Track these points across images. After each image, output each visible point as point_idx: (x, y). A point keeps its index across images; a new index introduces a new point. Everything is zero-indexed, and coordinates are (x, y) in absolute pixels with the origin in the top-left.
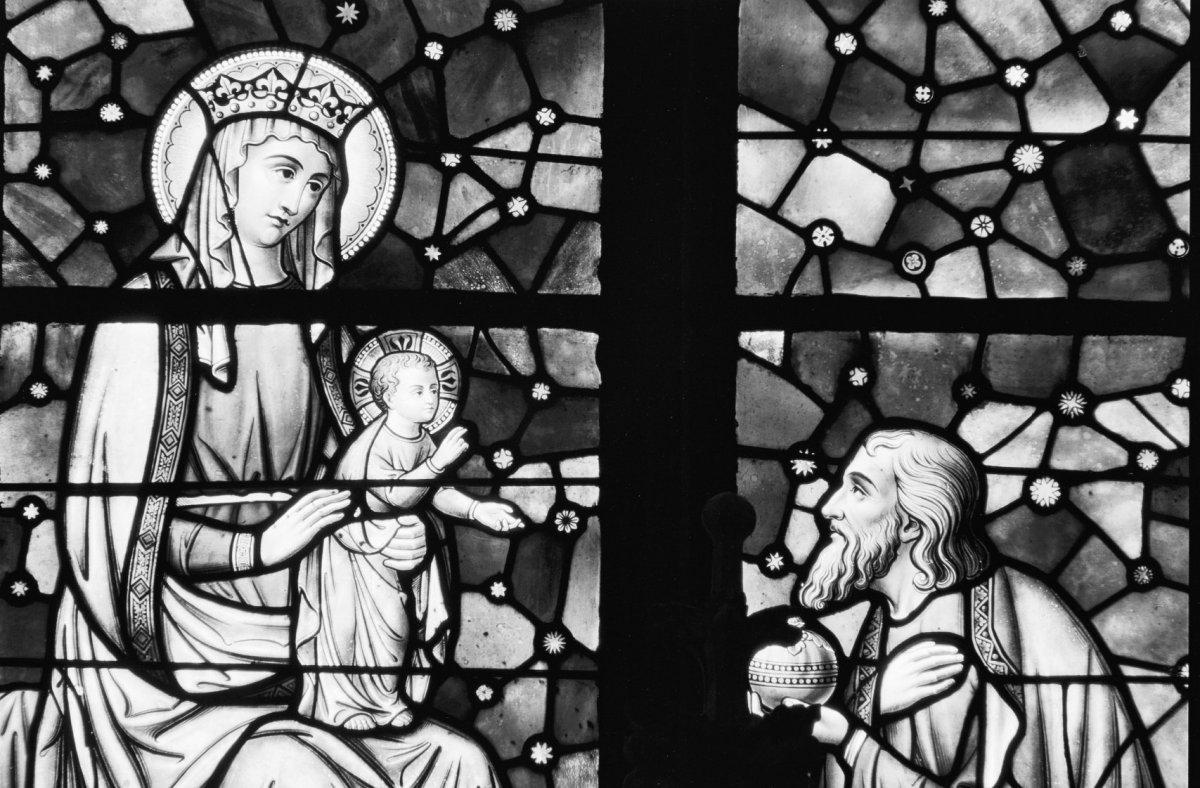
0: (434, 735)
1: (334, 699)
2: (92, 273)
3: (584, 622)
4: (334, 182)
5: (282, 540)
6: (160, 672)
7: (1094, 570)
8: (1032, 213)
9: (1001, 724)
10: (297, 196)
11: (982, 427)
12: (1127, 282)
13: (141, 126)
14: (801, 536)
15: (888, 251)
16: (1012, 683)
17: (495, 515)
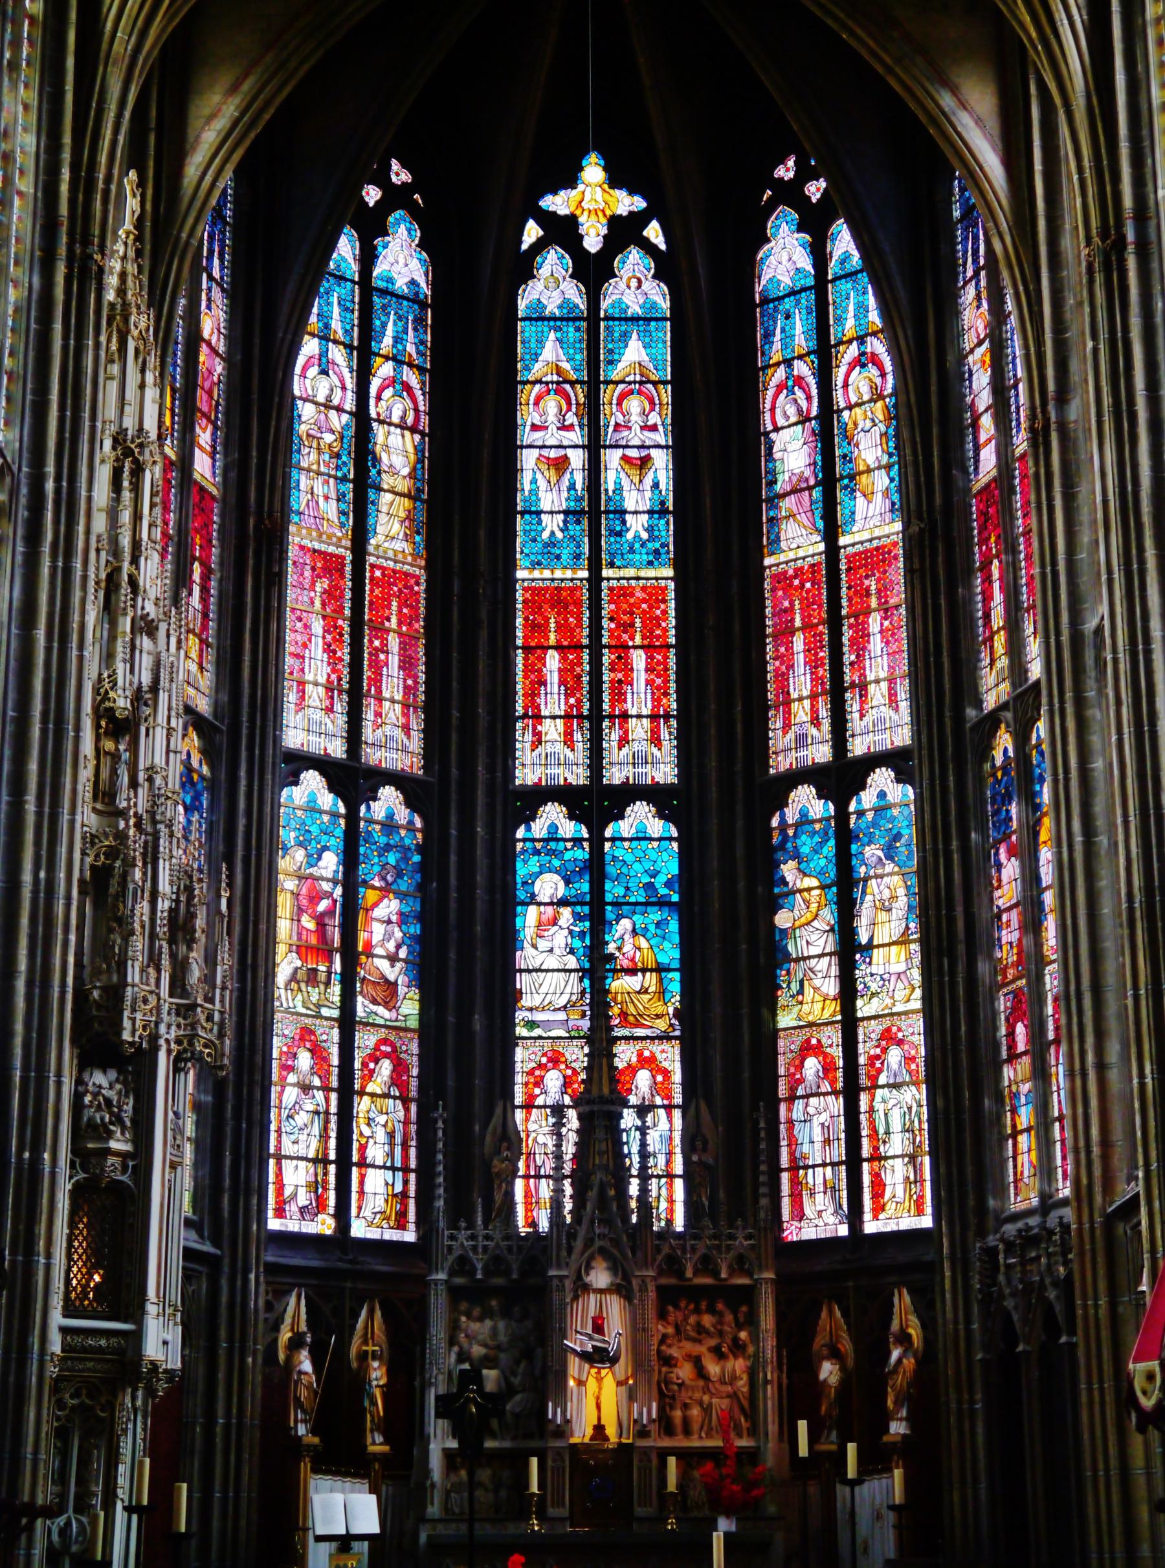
0: (570, 956)
1: (557, 951)
2: (528, 900)
3: (588, 942)
4: (556, 889)
5: (550, 932)
6: (536, 948)
7: (649, 935)
8: (642, 892)
9: (638, 953)
10: (552, 891)
11: (635, 918)
12: (652, 900)
13: (533, 883)
14: (613, 931)
15: (624, 897)
16: (639, 949)
17: (577, 929)
